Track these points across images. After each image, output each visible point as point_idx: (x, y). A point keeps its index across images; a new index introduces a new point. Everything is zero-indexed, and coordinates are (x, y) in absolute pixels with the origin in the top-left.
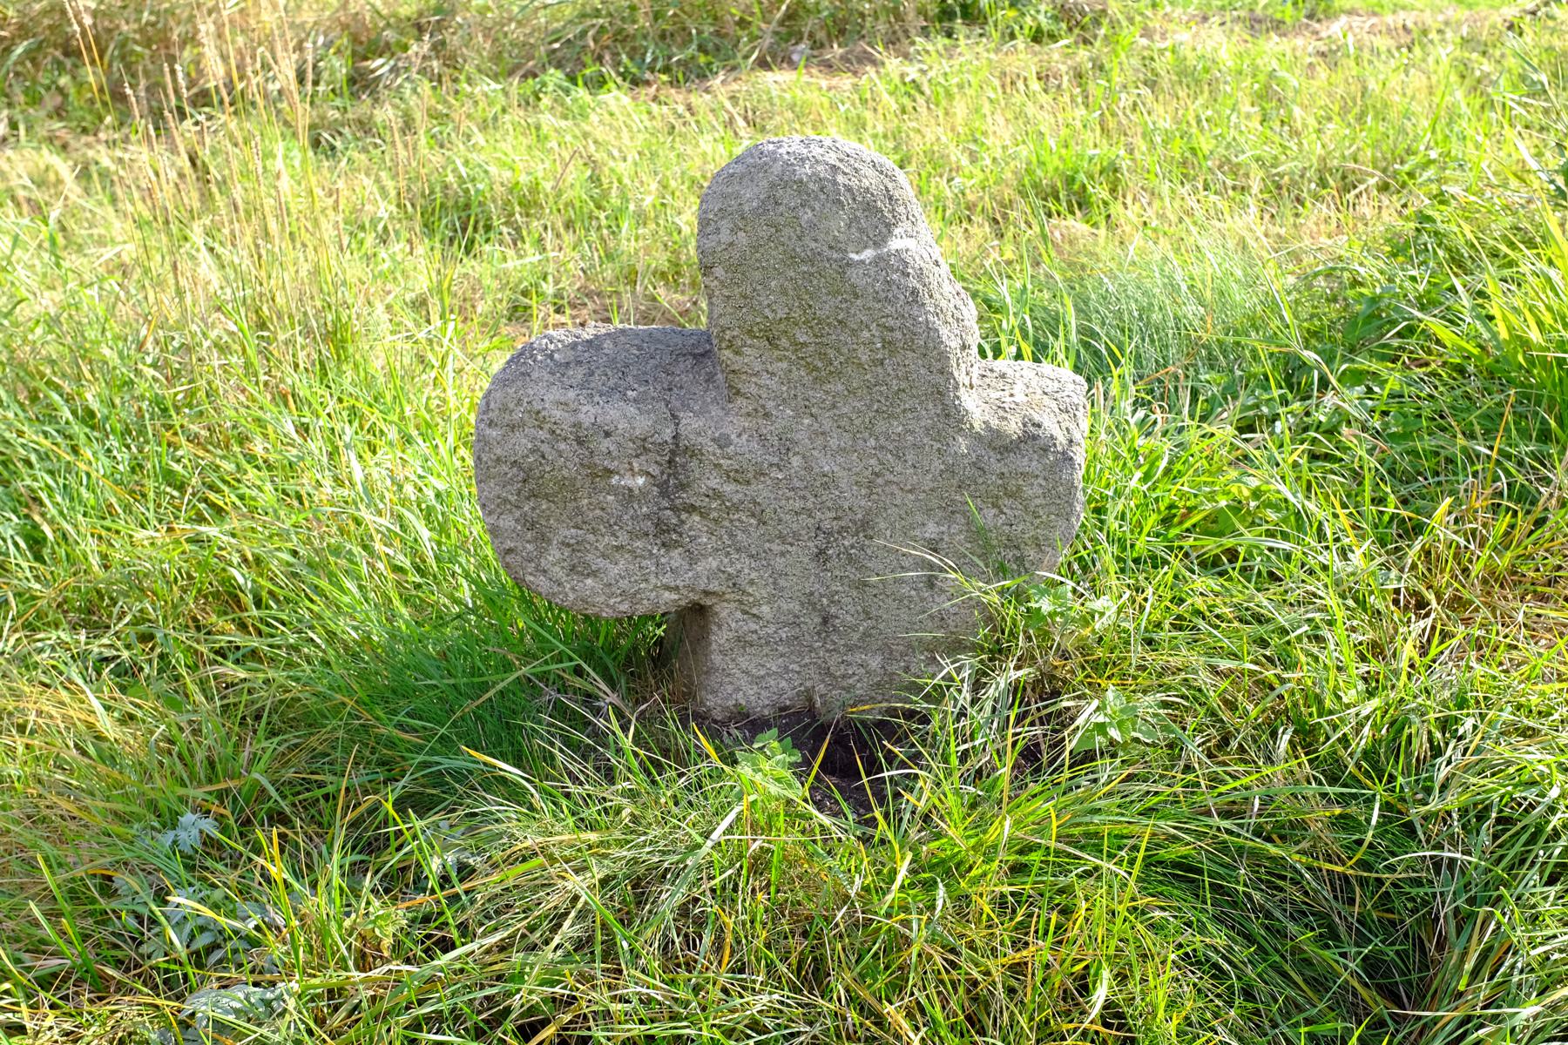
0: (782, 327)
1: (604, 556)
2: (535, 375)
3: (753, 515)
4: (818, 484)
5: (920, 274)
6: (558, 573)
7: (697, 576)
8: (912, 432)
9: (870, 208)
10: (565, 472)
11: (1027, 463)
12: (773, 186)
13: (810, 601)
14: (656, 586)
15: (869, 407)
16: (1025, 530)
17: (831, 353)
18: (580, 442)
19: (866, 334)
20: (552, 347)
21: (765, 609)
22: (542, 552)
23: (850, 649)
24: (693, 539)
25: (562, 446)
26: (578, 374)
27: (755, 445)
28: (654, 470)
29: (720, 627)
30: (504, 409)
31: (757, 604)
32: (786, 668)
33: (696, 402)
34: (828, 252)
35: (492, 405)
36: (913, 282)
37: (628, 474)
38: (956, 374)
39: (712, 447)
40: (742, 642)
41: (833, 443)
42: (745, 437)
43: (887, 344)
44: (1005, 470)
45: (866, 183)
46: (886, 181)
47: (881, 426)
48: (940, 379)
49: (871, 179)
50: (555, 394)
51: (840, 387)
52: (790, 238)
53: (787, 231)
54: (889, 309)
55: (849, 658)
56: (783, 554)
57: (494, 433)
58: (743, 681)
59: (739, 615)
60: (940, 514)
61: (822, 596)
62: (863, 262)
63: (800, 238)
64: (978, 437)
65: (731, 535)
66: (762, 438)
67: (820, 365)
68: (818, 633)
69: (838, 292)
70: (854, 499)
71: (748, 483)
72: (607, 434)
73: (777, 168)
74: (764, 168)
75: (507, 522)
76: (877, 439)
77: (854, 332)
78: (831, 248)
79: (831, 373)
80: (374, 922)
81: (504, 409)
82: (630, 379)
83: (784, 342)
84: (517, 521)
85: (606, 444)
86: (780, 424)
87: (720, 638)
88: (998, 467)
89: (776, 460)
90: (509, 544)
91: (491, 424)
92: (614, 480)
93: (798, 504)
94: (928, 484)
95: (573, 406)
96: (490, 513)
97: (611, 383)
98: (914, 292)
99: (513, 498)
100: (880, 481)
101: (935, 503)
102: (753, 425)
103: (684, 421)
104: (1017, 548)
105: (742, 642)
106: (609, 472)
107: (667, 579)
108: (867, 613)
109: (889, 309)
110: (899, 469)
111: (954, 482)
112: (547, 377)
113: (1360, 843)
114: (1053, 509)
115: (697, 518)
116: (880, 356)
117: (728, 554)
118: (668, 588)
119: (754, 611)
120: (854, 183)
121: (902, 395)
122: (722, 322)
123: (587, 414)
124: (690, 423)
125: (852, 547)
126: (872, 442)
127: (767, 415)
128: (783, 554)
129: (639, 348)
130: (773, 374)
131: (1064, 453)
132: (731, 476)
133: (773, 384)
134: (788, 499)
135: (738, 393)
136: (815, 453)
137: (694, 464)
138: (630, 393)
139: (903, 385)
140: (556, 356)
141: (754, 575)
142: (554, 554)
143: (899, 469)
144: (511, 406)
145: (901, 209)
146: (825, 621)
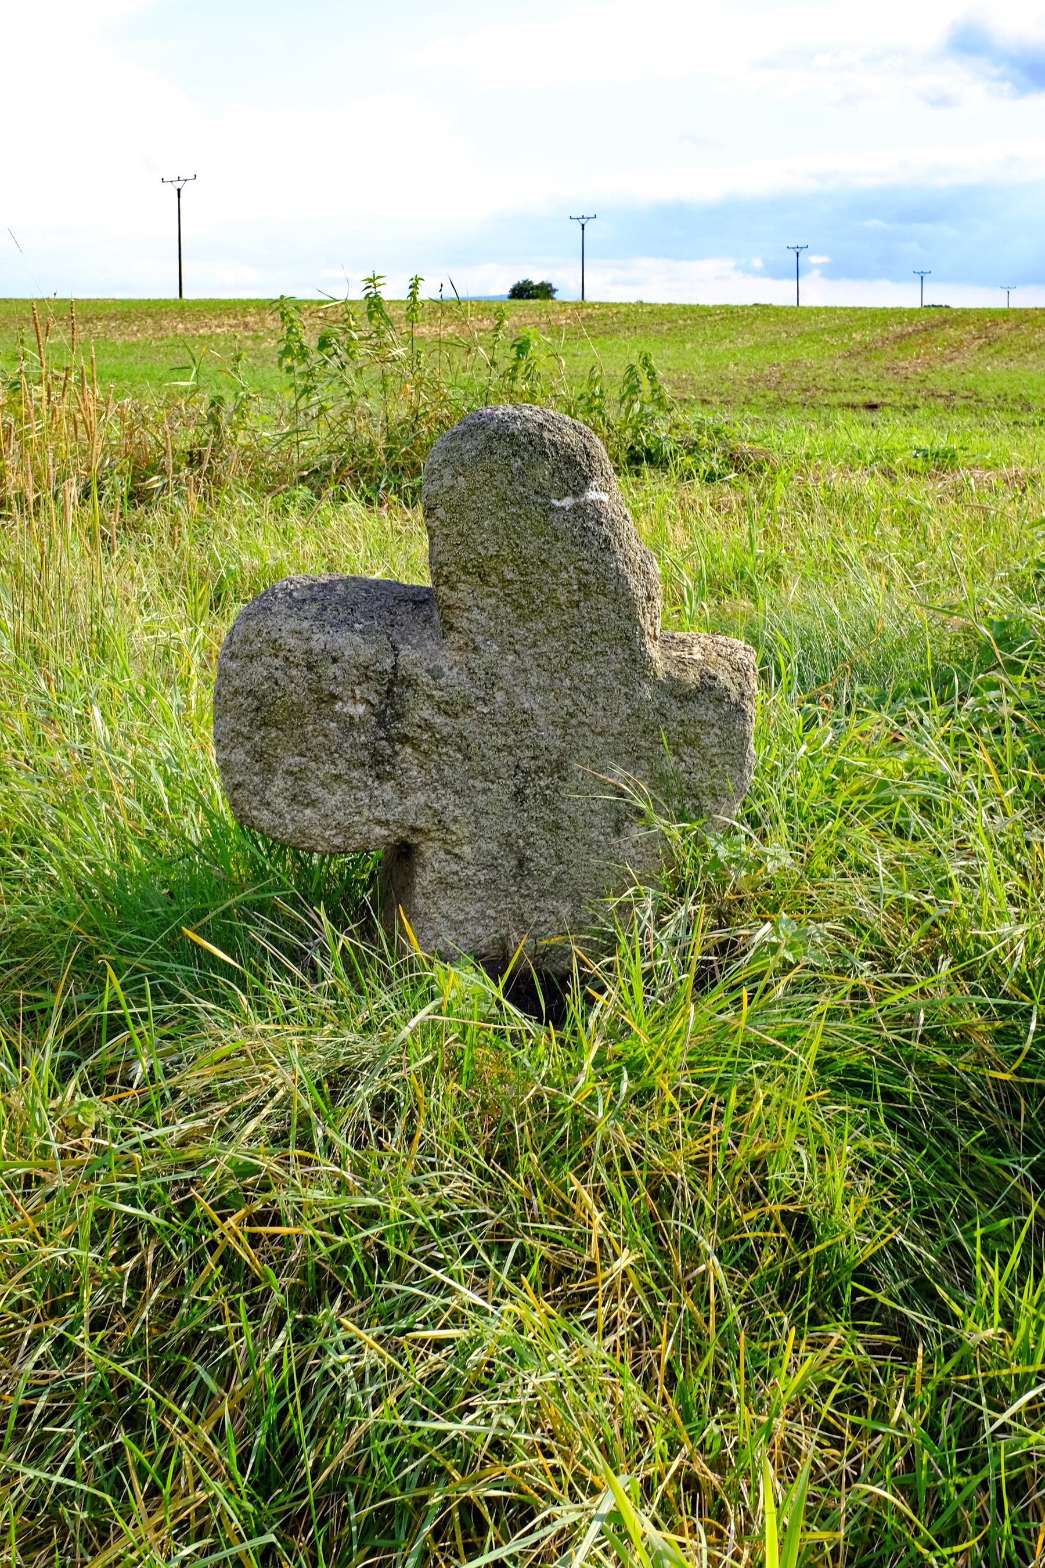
0: (492, 564)
1: (323, 785)
2: (275, 609)
3: (460, 750)
4: (518, 720)
5: (612, 524)
6: (280, 804)
7: (406, 811)
8: (603, 675)
9: (570, 461)
10: (294, 698)
11: (704, 712)
12: (490, 439)
13: (507, 842)
14: (368, 820)
15: (566, 647)
16: (702, 779)
17: (534, 592)
18: (310, 667)
19: (564, 575)
20: (292, 587)
21: (466, 849)
22: (267, 784)
23: (543, 894)
24: (405, 771)
25: (294, 672)
26: (315, 607)
27: (464, 677)
28: (374, 699)
29: (424, 868)
30: (246, 640)
31: (459, 843)
32: (483, 912)
33: (414, 637)
34: (533, 497)
35: (235, 639)
36: (606, 531)
37: (351, 701)
38: (642, 622)
39: (426, 678)
40: (443, 883)
41: (533, 680)
42: (456, 670)
43: (583, 586)
44: (684, 718)
45: (567, 440)
46: (585, 441)
47: (575, 667)
48: (628, 625)
49: (571, 438)
50: (293, 624)
51: (541, 626)
52: (502, 483)
53: (500, 476)
54: (585, 554)
55: (541, 904)
56: (485, 791)
57: (234, 665)
58: (443, 926)
59: (442, 855)
60: (627, 758)
61: (519, 837)
62: (563, 508)
63: (510, 483)
64: (661, 685)
65: (439, 770)
66: (471, 672)
67: (524, 602)
68: (514, 877)
69: (541, 534)
70: (550, 738)
71: (457, 716)
72: (335, 660)
73: (493, 425)
74: (482, 426)
75: (239, 756)
76: (572, 680)
77: (554, 574)
78: (536, 493)
79: (533, 611)
80: (78, 1109)
81: (246, 640)
82: (358, 614)
83: (493, 579)
84: (247, 753)
85: (333, 669)
86: (487, 658)
87: (424, 879)
88: (678, 714)
89: (482, 694)
90: (239, 778)
91: (233, 656)
92: (337, 707)
93: (500, 741)
94: (616, 728)
95: (306, 635)
96: (224, 748)
97: (341, 617)
98: (606, 540)
99: (244, 730)
100: (574, 722)
101: (622, 747)
102: (463, 659)
103: (403, 653)
104: (696, 797)
105: (443, 883)
106: (334, 698)
107: (379, 813)
108: (559, 857)
109: (585, 554)
110: (590, 710)
111: (640, 727)
112: (285, 610)
113: (1018, 1052)
114: (727, 758)
115: (409, 750)
116: (576, 598)
117: (435, 789)
118: (379, 823)
119: (456, 850)
120: (558, 438)
121: (595, 638)
122: (441, 558)
123: (319, 641)
124: (408, 655)
125: (548, 787)
126: (567, 682)
127: (476, 649)
128: (485, 791)
129: (367, 591)
130: (483, 609)
131: (736, 705)
132: (445, 708)
133: (482, 618)
134: (491, 734)
135: (452, 628)
136: (517, 689)
137: (409, 694)
138: (356, 626)
139: (596, 628)
140: (295, 594)
141: (457, 812)
142: (279, 783)
143: (590, 710)
144: (252, 637)
145: (596, 465)
146: (521, 864)
